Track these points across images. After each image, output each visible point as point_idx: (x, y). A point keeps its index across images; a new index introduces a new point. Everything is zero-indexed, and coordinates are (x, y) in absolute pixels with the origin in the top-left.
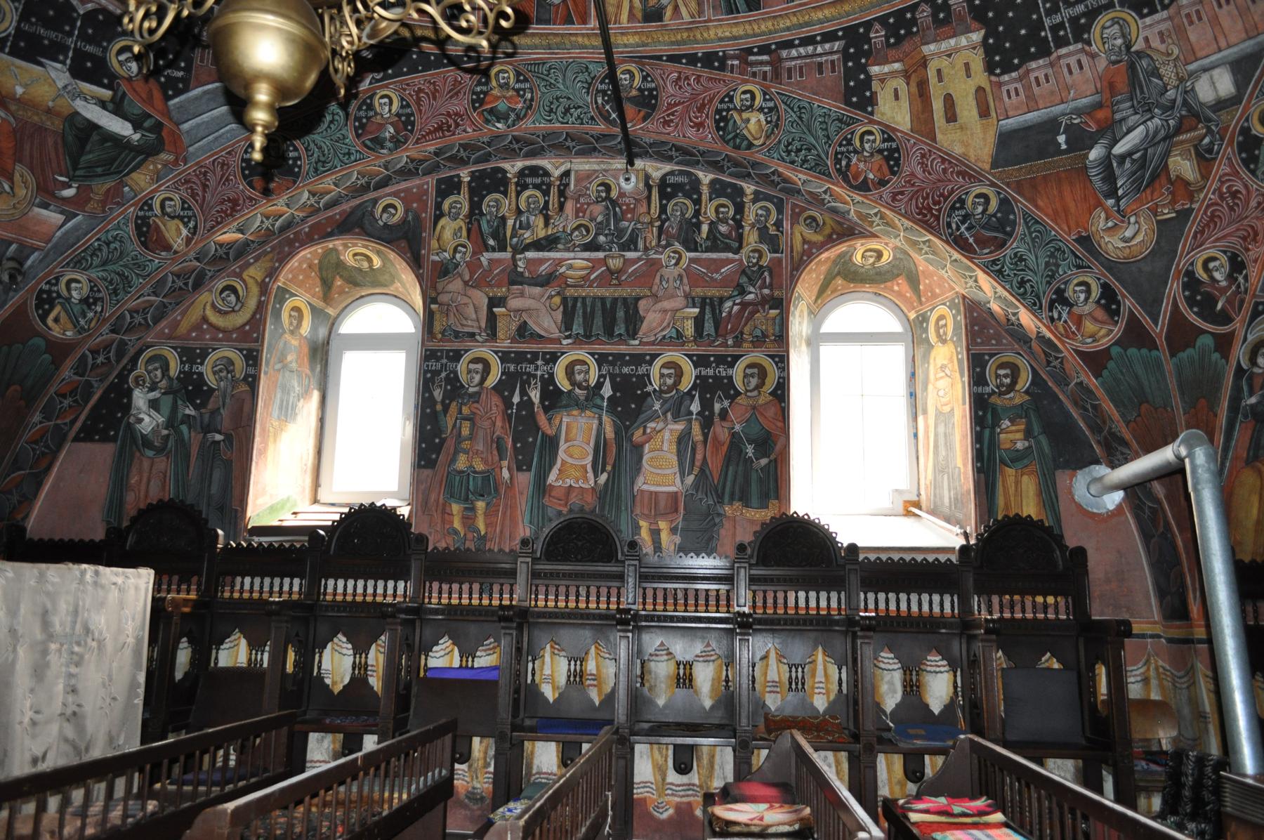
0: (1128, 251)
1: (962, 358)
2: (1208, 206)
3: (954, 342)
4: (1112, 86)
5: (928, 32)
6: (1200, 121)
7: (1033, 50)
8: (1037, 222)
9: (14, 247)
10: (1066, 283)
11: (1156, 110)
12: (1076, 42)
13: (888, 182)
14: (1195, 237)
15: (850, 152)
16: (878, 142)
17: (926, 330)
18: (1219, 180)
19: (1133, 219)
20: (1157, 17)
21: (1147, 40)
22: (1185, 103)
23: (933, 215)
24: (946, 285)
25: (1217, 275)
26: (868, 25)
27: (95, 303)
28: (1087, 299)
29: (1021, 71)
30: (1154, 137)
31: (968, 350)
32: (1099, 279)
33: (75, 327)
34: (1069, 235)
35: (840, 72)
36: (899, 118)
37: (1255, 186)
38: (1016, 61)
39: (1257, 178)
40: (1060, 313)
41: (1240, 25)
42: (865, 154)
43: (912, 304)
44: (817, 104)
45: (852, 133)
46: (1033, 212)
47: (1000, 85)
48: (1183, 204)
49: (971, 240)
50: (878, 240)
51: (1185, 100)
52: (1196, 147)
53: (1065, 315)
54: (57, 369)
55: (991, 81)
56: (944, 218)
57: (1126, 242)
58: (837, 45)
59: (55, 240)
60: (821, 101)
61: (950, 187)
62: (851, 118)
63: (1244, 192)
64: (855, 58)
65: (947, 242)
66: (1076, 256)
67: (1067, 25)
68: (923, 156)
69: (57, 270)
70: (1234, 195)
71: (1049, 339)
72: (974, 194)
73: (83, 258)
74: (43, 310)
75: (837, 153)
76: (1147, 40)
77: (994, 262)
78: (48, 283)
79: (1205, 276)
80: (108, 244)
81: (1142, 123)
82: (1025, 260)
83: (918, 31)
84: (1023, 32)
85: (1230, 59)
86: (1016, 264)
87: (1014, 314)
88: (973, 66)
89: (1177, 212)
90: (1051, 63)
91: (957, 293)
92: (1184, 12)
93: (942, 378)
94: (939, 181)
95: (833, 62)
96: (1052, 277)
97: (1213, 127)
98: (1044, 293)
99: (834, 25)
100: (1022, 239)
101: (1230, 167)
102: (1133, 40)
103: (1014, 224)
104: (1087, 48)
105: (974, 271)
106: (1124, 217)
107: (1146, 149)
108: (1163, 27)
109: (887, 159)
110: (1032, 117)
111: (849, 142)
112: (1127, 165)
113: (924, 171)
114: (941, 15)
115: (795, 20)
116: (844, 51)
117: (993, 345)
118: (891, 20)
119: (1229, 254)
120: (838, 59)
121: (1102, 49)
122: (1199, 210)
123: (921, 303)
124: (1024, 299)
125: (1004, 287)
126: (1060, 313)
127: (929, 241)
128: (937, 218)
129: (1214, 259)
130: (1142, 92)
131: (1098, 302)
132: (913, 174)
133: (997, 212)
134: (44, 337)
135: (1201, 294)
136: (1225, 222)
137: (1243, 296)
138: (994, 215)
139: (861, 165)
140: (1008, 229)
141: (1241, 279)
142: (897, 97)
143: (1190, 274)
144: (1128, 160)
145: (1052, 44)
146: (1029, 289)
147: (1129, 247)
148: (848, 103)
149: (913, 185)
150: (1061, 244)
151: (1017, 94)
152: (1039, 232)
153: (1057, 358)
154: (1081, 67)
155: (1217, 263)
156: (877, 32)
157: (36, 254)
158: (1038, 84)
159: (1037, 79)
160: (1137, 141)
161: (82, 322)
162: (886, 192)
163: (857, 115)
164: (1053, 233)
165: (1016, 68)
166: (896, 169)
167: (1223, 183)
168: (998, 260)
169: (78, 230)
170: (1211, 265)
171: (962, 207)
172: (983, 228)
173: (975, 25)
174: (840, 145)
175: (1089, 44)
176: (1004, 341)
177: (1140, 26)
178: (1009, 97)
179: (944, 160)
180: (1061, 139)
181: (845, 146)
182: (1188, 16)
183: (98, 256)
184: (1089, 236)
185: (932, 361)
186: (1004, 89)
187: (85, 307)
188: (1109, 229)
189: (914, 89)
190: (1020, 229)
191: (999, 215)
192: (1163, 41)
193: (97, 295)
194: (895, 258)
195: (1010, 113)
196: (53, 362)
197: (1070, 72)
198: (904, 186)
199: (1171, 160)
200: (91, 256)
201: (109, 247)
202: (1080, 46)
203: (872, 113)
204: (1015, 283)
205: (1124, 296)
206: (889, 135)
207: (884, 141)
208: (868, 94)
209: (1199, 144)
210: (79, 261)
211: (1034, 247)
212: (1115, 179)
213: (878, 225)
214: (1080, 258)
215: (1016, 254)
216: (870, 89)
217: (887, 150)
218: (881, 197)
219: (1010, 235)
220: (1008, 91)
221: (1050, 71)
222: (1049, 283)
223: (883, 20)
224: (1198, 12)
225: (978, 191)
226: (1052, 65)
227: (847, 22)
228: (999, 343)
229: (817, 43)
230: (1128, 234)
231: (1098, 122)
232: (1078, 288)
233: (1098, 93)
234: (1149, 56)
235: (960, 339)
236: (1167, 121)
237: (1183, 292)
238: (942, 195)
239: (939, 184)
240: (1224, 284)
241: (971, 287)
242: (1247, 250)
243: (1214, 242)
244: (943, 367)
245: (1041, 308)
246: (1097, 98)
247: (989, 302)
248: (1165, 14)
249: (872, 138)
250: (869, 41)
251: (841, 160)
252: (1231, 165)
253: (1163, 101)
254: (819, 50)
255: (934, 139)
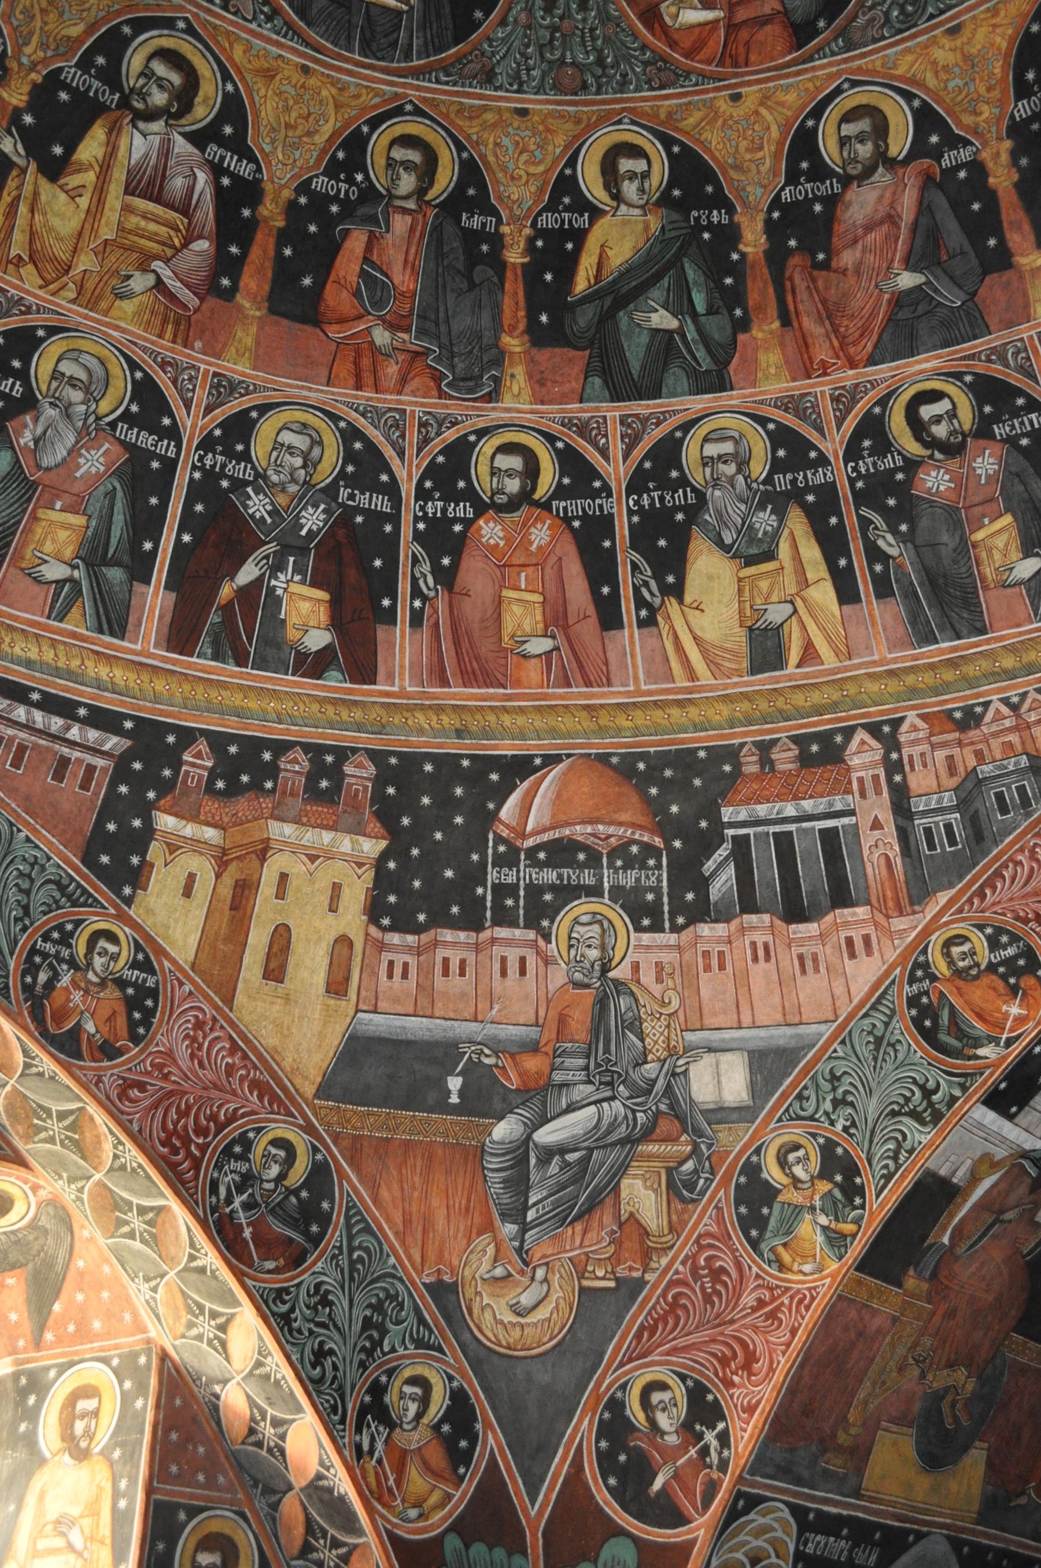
0: (516, 1333)
1: (130, 1509)
2: (672, 1284)
3: (111, 1464)
4: (562, 1020)
5: (289, 800)
6: (685, 1131)
7: (455, 910)
8: (367, 1230)
10: (390, 1373)
11: (621, 1088)
12: (526, 927)
13: (120, 1052)
14: (638, 1336)
15: (61, 960)
16: (122, 962)
17: (32, 1415)
18: (697, 1241)
19: (540, 1273)
20: (660, 938)
21: (636, 967)
22: (669, 1089)
23: (189, 1154)
24: (128, 1317)
25: (663, 1421)
26: (187, 736)
28: (419, 1416)
29: (425, 937)
30: (608, 1132)
31: (149, 1491)
32: (451, 1378)
34: (420, 1273)
35: (96, 794)
36: (177, 933)
37: (755, 1269)
38: (422, 917)
39: (761, 1255)
40: (373, 1440)
41: (777, 999)
42: (91, 976)
43: (13, 1339)
44: (25, 832)
45: (78, 923)
46: (367, 1209)
47: (381, 947)
48: (631, 1269)
49: (247, 1233)
50: (23, 1172)
51: (669, 1086)
52: (669, 1171)
53: (380, 1446)
55: (367, 934)
56: (207, 1171)
57: (519, 1314)
58: (112, 742)
60: (35, 831)
61: (232, 1106)
62: (85, 891)
63: (734, 1274)
64: (139, 783)
65: (203, 1224)
66: (422, 1321)
67: (522, 893)
68: (199, 1025)
70: (717, 1274)
71: (342, 1499)
72: (270, 1136)
75: (33, 951)
76: (636, 967)
77: (280, 1294)
79: (641, 1416)
81: (595, 1103)
82: (331, 1304)
83: (274, 790)
84: (449, 873)
85: (751, 1046)
86: (315, 1309)
87: (276, 1423)
88: (346, 893)
89: (617, 1279)
90: (477, 944)
91: (148, 1341)
92: (701, 948)
93: (52, 1552)
94: (216, 1086)
95: (91, 769)
96: (369, 1352)
97: (703, 1147)
98: (353, 1387)
99: (122, 703)
100: (334, 1257)
101: (718, 1224)
102: (614, 964)
103: (325, 1220)
104: (541, 943)
105: (236, 1303)
106: (526, 1264)
107: (590, 1150)
108: (666, 957)
109: (132, 1004)
110: (417, 1027)
111: (66, 939)
112: (554, 1168)
113: (192, 1056)
114: (324, 784)
115: (49, 655)
116: (122, 763)
117: (198, 1486)
118: (233, 749)
119: (690, 1383)
120: (104, 770)
121: (564, 954)
122: (655, 1287)
123: (38, 1343)
124: (319, 1393)
125: (288, 1357)
126: (373, 1440)
127: (160, 1210)
128: (197, 1167)
129: (663, 1386)
130: (606, 1050)
131: (436, 1428)
132: (170, 1054)
133: (301, 1187)
135: (628, 1451)
136: (693, 1322)
137: (715, 1475)
138: (296, 1192)
139: (77, 996)
140: (314, 1228)
141: (710, 1438)
142: (188, 892)
143: (616, 1406)
144: (556, 1159)
145: (488, 914)
146: (329, 1374)
147: (522, 1326)
148: (89, 859)
149: (166, 1077)
150: (400, 1286)
151: (405, 975)
152: (367, 1250)
153: (336, 1544)
154: (523, 972)
155: (666, 1396)
156: (199, 755)
158: (446, 973)
159: (446, 961)
160: (579, 1131)
162: (112, 1071)
163: (100, 891)
164: (392, 1260)
165: (418, 930)
166: (141, 1031)
167: (701, 1248)
168: (287, 1291)
170: (656, 1397)
171: (244, 1157)
172: (272, 1211)
173: (374, 826)
174: (46, 937)
175: (547, 937)
176: (221, 1479)
177: (632, 942)
178: (390, 976)
179: (234, 1048)
180: (455, 1083)
181: (55, 942)
182: (706, 954)
184: (456, 1283)
185: (31, 1499)
186: (386, 957)
188: (496, 1279)
189: (226, 891)
190: (335, 1235)
191: (304, 1194)
192: (659, 980)
194: (33, 1226)
195: (382, 1005)
197: (504, 973)
198: (147, 1073)
199: (625, 1183)
202: (531, 935)
203: (129, 901)
204: (308, 1350)
205: (487, 1425)
206: (147, 958)
207: (135, 965)
208: (135, 860)
209: (676, 1168)
211: (352, 1279)
212: (528, 1188)
213: (51, 1140)
214: (426, 1325)
215: (318, 1286)
216: (143, 854)
217: (134, 985)
218: (100, 1080)
219: (316, 1240)
220: (391, 963)
221: (471, 958)
222: (363, 1365)
223: (218, 741)
224: (721, 954)
225: (279, 1133)
226: (477, 948)
227: (152, 711)
228: (210, 1483)
229: (76, 719)
230: (526, 1300)
231: (522, 1074)
232: (408, 1389)
233: (537, 1025)
234: (632, 994)
235: (131, 1457)
236: (634, 1111)
237: (597, 1441)
238: (213, 1117)
239: (214, 1093)
240: (672, 1439)
241: (199, 1338)
242: (729, 1384)
243: (668, 1353)
244: (62, 1524)
245: (343, 1421)
246: (533, 1032)
247: (225, 1382)
248: (672, 938)
249: (112, 948)
250: (176, 764)
251: (38, 968)
252: (720, 1220)
253: (635, 1076)
254: (74, 733)
255: (229, 1000)
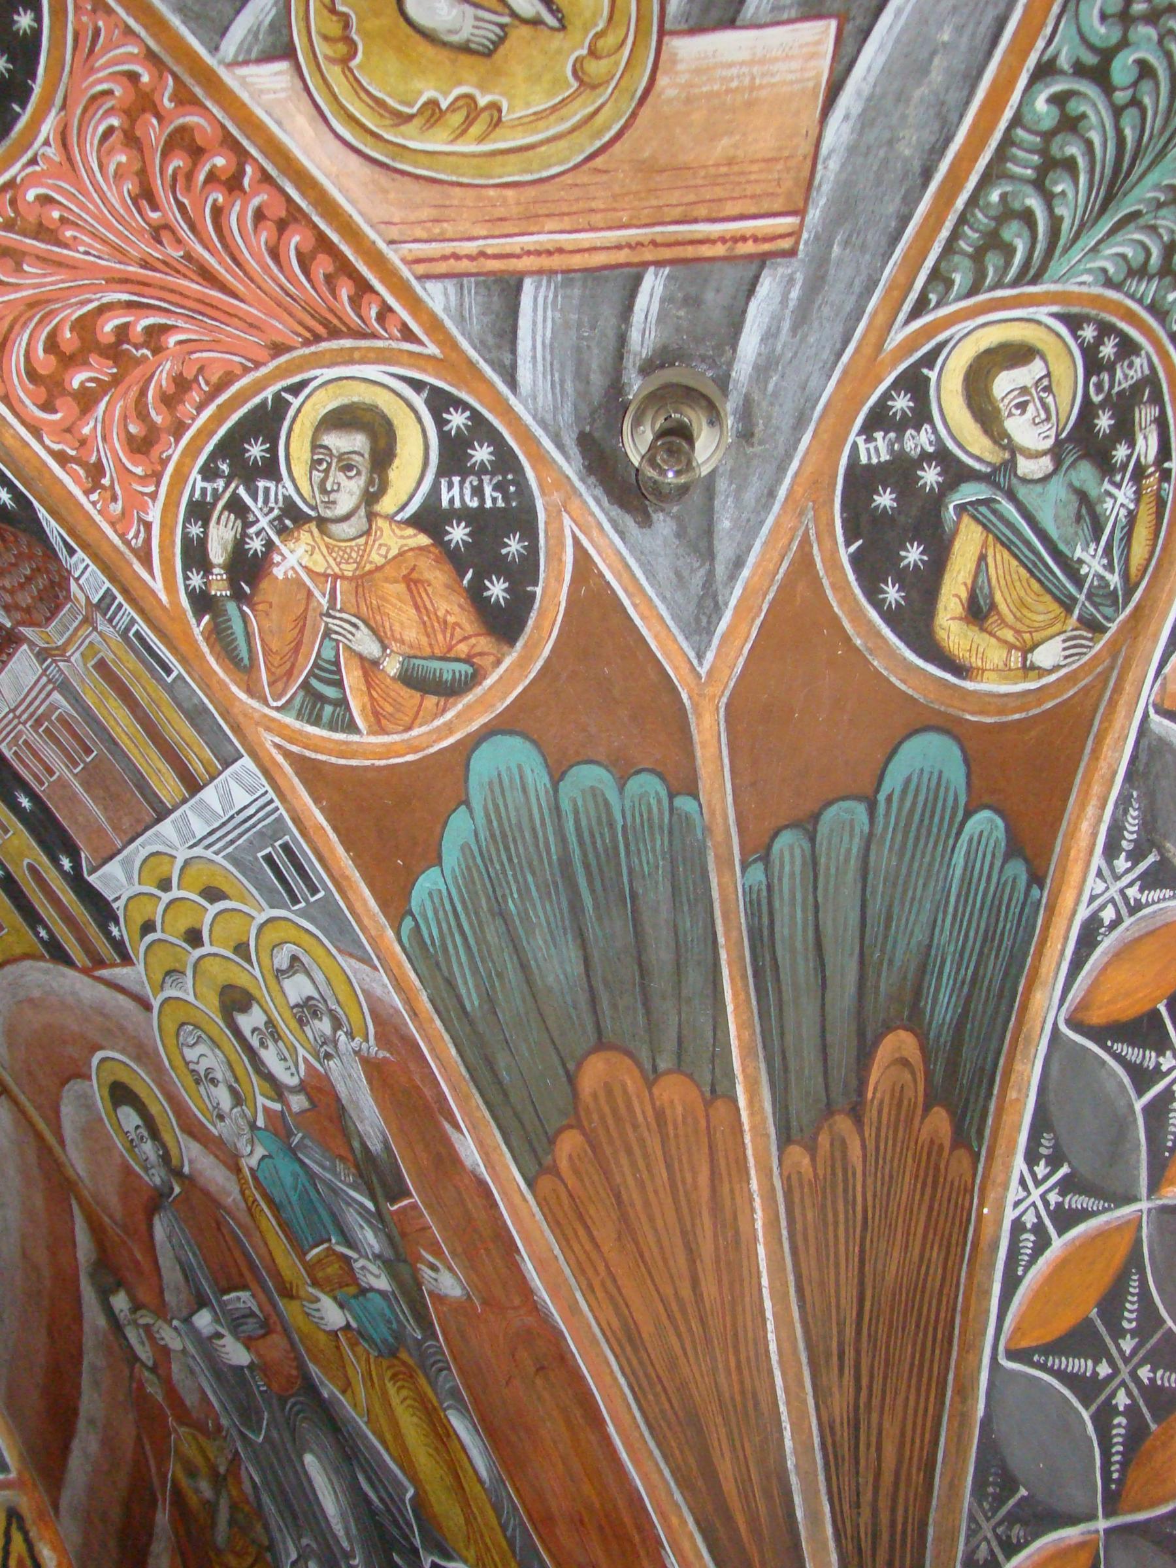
9: (652, 286)
27: (1125, 431)
33: (1067, 604)
54: (1037, 879)
59: (829, 172)
69: (897, 336)
73: (1008, 213)
74: (903, 578)
78: (879, 420)
80: (1100, 75)
134: (948, 727)
157: (767, 286)
161: (1092, 562)
169: (923, 70)
183: (1070, 165)
187: (1085, 474)
193: (1128, 375)
196: (1015, 848)
200: (1039, 184)
201: (1108, 88)
210: (993, 242)
